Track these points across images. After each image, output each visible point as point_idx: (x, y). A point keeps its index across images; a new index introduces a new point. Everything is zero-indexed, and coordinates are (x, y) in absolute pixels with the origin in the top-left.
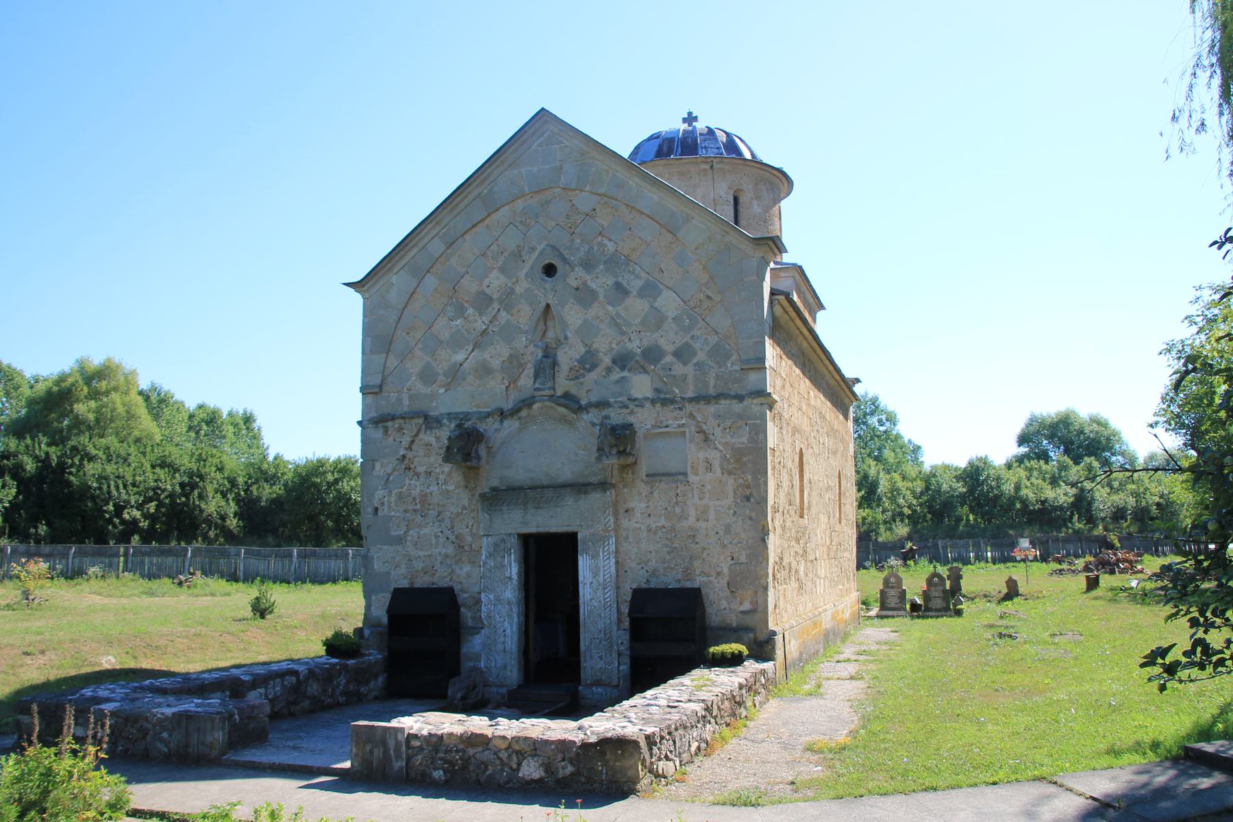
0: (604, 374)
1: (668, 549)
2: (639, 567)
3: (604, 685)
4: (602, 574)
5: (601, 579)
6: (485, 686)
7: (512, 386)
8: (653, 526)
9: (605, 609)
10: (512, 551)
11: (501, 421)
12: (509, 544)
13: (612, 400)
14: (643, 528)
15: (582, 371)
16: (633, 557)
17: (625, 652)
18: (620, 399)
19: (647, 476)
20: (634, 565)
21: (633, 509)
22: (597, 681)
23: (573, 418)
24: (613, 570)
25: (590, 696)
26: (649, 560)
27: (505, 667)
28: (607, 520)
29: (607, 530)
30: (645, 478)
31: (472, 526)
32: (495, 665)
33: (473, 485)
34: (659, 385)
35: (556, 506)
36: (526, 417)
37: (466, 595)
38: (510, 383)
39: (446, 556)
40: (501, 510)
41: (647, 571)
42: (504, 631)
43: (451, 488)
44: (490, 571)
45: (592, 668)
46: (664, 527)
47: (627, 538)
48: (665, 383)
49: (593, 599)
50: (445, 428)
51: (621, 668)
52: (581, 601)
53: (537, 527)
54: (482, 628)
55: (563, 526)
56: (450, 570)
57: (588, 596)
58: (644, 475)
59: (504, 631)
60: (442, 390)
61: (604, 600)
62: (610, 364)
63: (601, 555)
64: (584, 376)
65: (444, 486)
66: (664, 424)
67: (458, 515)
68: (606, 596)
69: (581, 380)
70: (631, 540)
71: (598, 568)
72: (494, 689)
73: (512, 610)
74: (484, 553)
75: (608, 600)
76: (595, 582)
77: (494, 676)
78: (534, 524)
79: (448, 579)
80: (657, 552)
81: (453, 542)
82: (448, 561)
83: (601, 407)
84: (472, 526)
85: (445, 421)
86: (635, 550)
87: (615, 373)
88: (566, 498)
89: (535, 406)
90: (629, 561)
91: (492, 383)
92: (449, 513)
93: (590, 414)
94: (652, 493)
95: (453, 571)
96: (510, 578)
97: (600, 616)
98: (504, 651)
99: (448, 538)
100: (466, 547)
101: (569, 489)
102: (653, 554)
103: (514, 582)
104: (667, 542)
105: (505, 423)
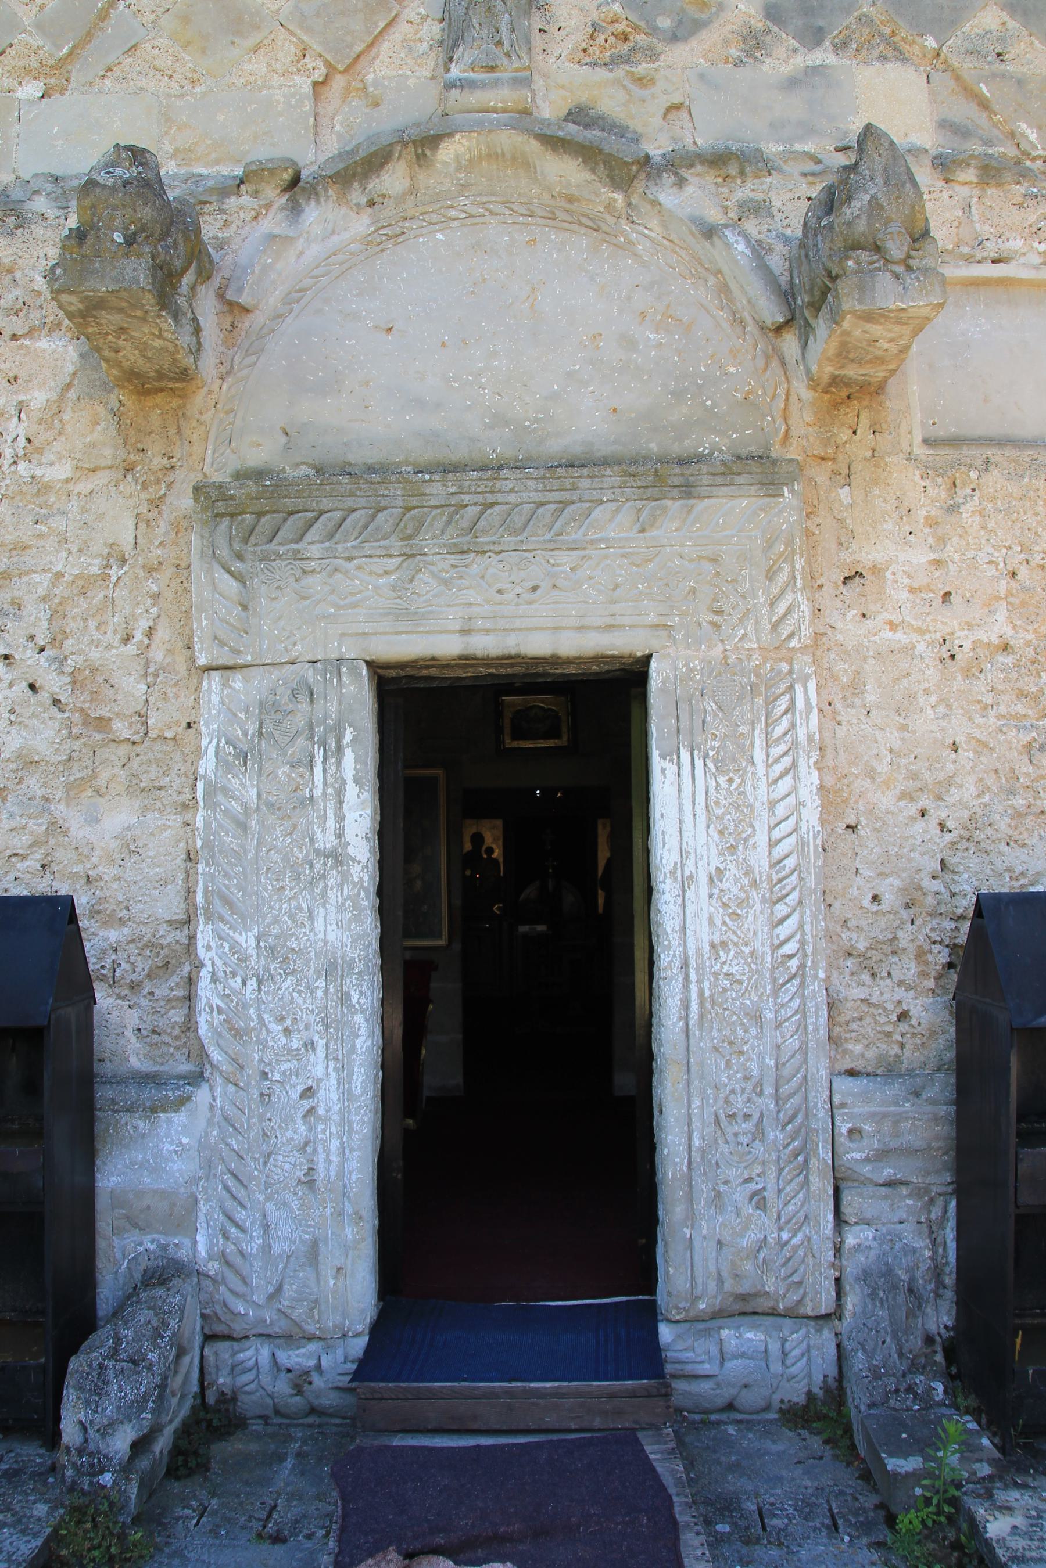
0: (734, 52)
1: (1025, 738)
2: (913, 810)
3: (773, 1313)
4: (761, 839)
5: (759, 860)
6: (210, 1338)
7: (339, 82)
8: (965, 639)
9: (775, 993)
10: (348, 736)
11: (295, 209)
12: (333, 707)
13: (772, 148)
14: (921, 647)
15: (641, 38)
16: (883, 768)
17: (866, 1170)
18: (809, 147)
19: (926, 441)
20: (886, 800)
21: (877, 570)
22: (743, 1298)
23: (609, 207)
24: (811, 816)
25: (706, 1368)
26: (950, 782)
27: (313, 1253)
28: (781, 608)
29: (780, 650)
30: (920, 451)
31: (150, 632)
32: (266, 1248)
33: (158, 462)
34: (964, 111)
35: (553, 546)
36: (401, 199)
37: (113, 935)
38: (331, 68)
39: (27, 762)
40: (297, 556)
41: (942, 826)
42: (308, 1092)
43: (58, 472)
44: (244, 827)
45: (719, 1242)
46: (1006, 648)
47: (855, 687)
48: (984, 105)
49: (724, 944)
50: (38, 230)
51: (850, 1241)
52: (667, 959)
53: (465, 632)
54: (197, 1078)
55: (581, 628)
56: (38, 827)
57: (701, 935)
58: (918, 438)
59: (308, 1092)
60: (31, 90)
61: (775, 948)
62: (758, 23)
63: (759, 756)
64: (653, 56)
65: (22, 467)
66: (992, 249)
67: (84, 585)
68: (783, 931)
69: (642, 68)
70: (871, 698)
71: (742, 807)
72: (259, 1353)
73: (343, 998)
74: (209, 745)
75: (790, 948)
76: (733, 871)
77: (259, 1298)
78: (452, 619)
79: (32, 863)
80: (982, 746)
81: (56, 702)
82: (33, 783)
83: (733, 169)
84: (150, 632)
85: (40, 204)
86: (893, 738)
87: (780, 51)
88: (598, 513)
89: (447, 153)
90: (867, 783)
91: (257, 66)
92: (42, 582)
93: (689, 189)
94: (953, 509)
95: (55, 827)
96: (338, 857)
97: (758, 1018)
98: (309, 1183)
99: (32, 687)
100: (117, 725)
101: (611, 477)
102: (966, 754)
103: (356, 871)
104: (1020, 709)
105: (312, 214)
